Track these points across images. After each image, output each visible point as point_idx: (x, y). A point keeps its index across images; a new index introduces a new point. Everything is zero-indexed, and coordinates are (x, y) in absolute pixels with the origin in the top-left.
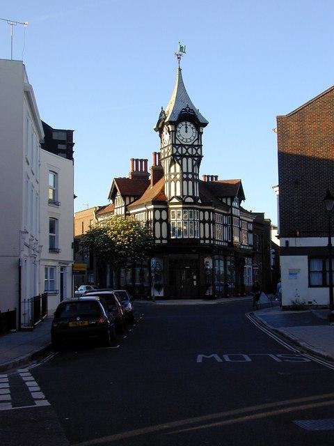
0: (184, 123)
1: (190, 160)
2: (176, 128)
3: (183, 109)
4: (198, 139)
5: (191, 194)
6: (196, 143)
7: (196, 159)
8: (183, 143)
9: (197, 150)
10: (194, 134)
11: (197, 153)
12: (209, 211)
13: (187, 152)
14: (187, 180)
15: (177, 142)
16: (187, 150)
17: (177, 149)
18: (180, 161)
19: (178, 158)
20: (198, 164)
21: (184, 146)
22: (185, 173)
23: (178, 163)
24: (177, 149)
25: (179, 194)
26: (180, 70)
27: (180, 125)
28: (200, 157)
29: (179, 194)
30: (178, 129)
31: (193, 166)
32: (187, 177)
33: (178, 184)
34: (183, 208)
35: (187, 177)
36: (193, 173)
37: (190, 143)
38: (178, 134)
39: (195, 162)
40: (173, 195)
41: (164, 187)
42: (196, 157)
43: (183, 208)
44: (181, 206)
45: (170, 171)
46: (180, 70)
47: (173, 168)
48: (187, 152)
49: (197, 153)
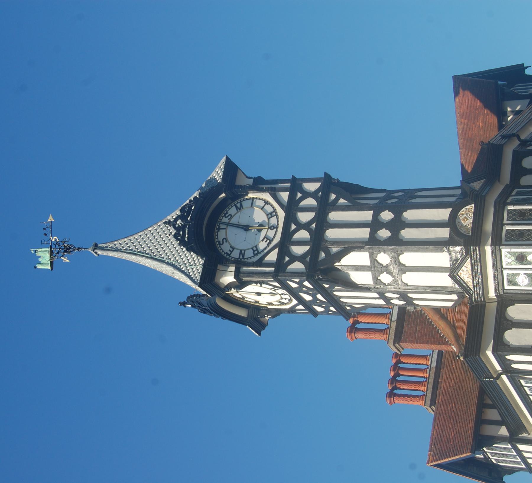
0: (221, 235)
1: (334, 216)
3: (176, 236)
5: (444, 214)
6: (285, 196)
7: (333, 196)
9: (306, 195)
11: (313, 195)
12: (518, 157)
13: (306, 226)
15: (273, 257)
16: (301, 226)
17: (294, 258)
18: (335, 249)
19: (323, 255)
21: (287, 235)
24: (294, 258)
27: (226, 248)
30: (236, 254)
32: (388, 225)
34: (497, 243)
35: (388, 225)
36: (377, 210)
37: (281, 214)
38: (249, 254)
39: (342, 201)
41: (437, 310)
42: (326, 196)
43: (497, 243)
44: (488, 249)
48: (306, 226)
49: (313, 195)
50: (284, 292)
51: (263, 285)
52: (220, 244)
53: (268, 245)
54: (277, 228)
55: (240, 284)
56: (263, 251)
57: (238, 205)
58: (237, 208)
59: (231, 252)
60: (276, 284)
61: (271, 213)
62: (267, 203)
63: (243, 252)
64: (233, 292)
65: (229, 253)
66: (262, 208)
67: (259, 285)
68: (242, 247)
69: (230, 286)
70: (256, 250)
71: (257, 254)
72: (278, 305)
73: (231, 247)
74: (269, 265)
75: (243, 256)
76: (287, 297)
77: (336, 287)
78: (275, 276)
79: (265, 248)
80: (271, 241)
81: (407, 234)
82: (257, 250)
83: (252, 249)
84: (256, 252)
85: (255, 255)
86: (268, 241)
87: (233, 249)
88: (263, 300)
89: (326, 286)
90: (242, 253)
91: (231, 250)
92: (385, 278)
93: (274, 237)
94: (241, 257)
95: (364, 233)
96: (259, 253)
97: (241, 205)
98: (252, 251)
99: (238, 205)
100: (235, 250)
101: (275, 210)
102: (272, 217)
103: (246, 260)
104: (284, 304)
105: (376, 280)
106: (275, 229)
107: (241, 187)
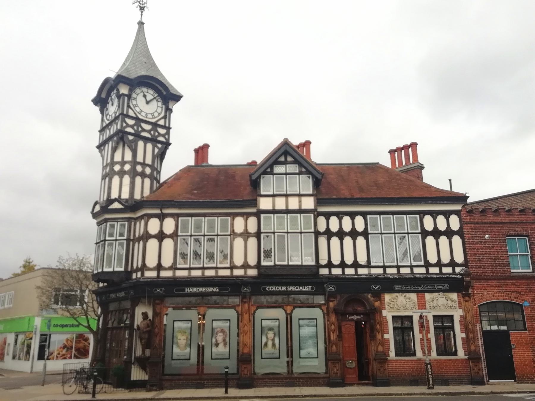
2: (131, 90)
4: (165, 117)
6: (162, 122)
7: (160, 146)
8: (140, 117)
10: (159, 110)
14: (143, 175)
20: (162, 156)
22: (140, 163)
23: (130, 147)
25: (125, 195)
26: (141, 24)
27: (138, 91)
28: (167, 144)
29: (125, 195)
30: (134, 95)
31: (154, 157)
33: (127, 179)
37: (153, 121)
38: (134, 102)
39: (156, 150)
40: (114, 195)
45: (112, 158)
46: (141, 24)
47: (118, 157)
50: (113, 118)
51: (117, 107)
52: (140, 88)
53: (138, 112)
54: (146, 117)
55: (119, 96)
56: (135, 109)
57: (159, 100)
58: (158, 99)
59: (136, 94)
60: (117, 114)
61: (154, 115)
62: (159, 114)
63: (135, 99)
64: (115, 91)
65: (135, 92)
66: (156, 111)
67: (118, 105)
68: (137, 99)
69: (118, 91)
70: (135, 106)
71: (134, 106)
72: (106, 113)
73: (138, 94)
74: (127, 112)
75: (134, 99)
76: (110, 118)
77: (114, 144)
78: (122, 114)
79: (136, 111)
80: (140, 114)
81: (138, 179)
82: (136, 106)
83: (137, 104)
84: (135, 106)
85: (133, 105)
86: (140, 112)
87: (137, 95)
88: (109, 106)
89: (115, 138)
90: (135, 99)
91: (137, 94)
92: (117, 168)
93: (142, 116)
94: (133, 98)
95: (140, 159)
96: (134, 107)
97: (159, 101)
98: (136, 104)
99: (159, 100)
100: (136, 95)
101: (155, 118)
102: (152, 116)
103: (130, 100)
104: (106, 116)
105: (117, 163)
106: (145, 116)
107: (168, 102)
